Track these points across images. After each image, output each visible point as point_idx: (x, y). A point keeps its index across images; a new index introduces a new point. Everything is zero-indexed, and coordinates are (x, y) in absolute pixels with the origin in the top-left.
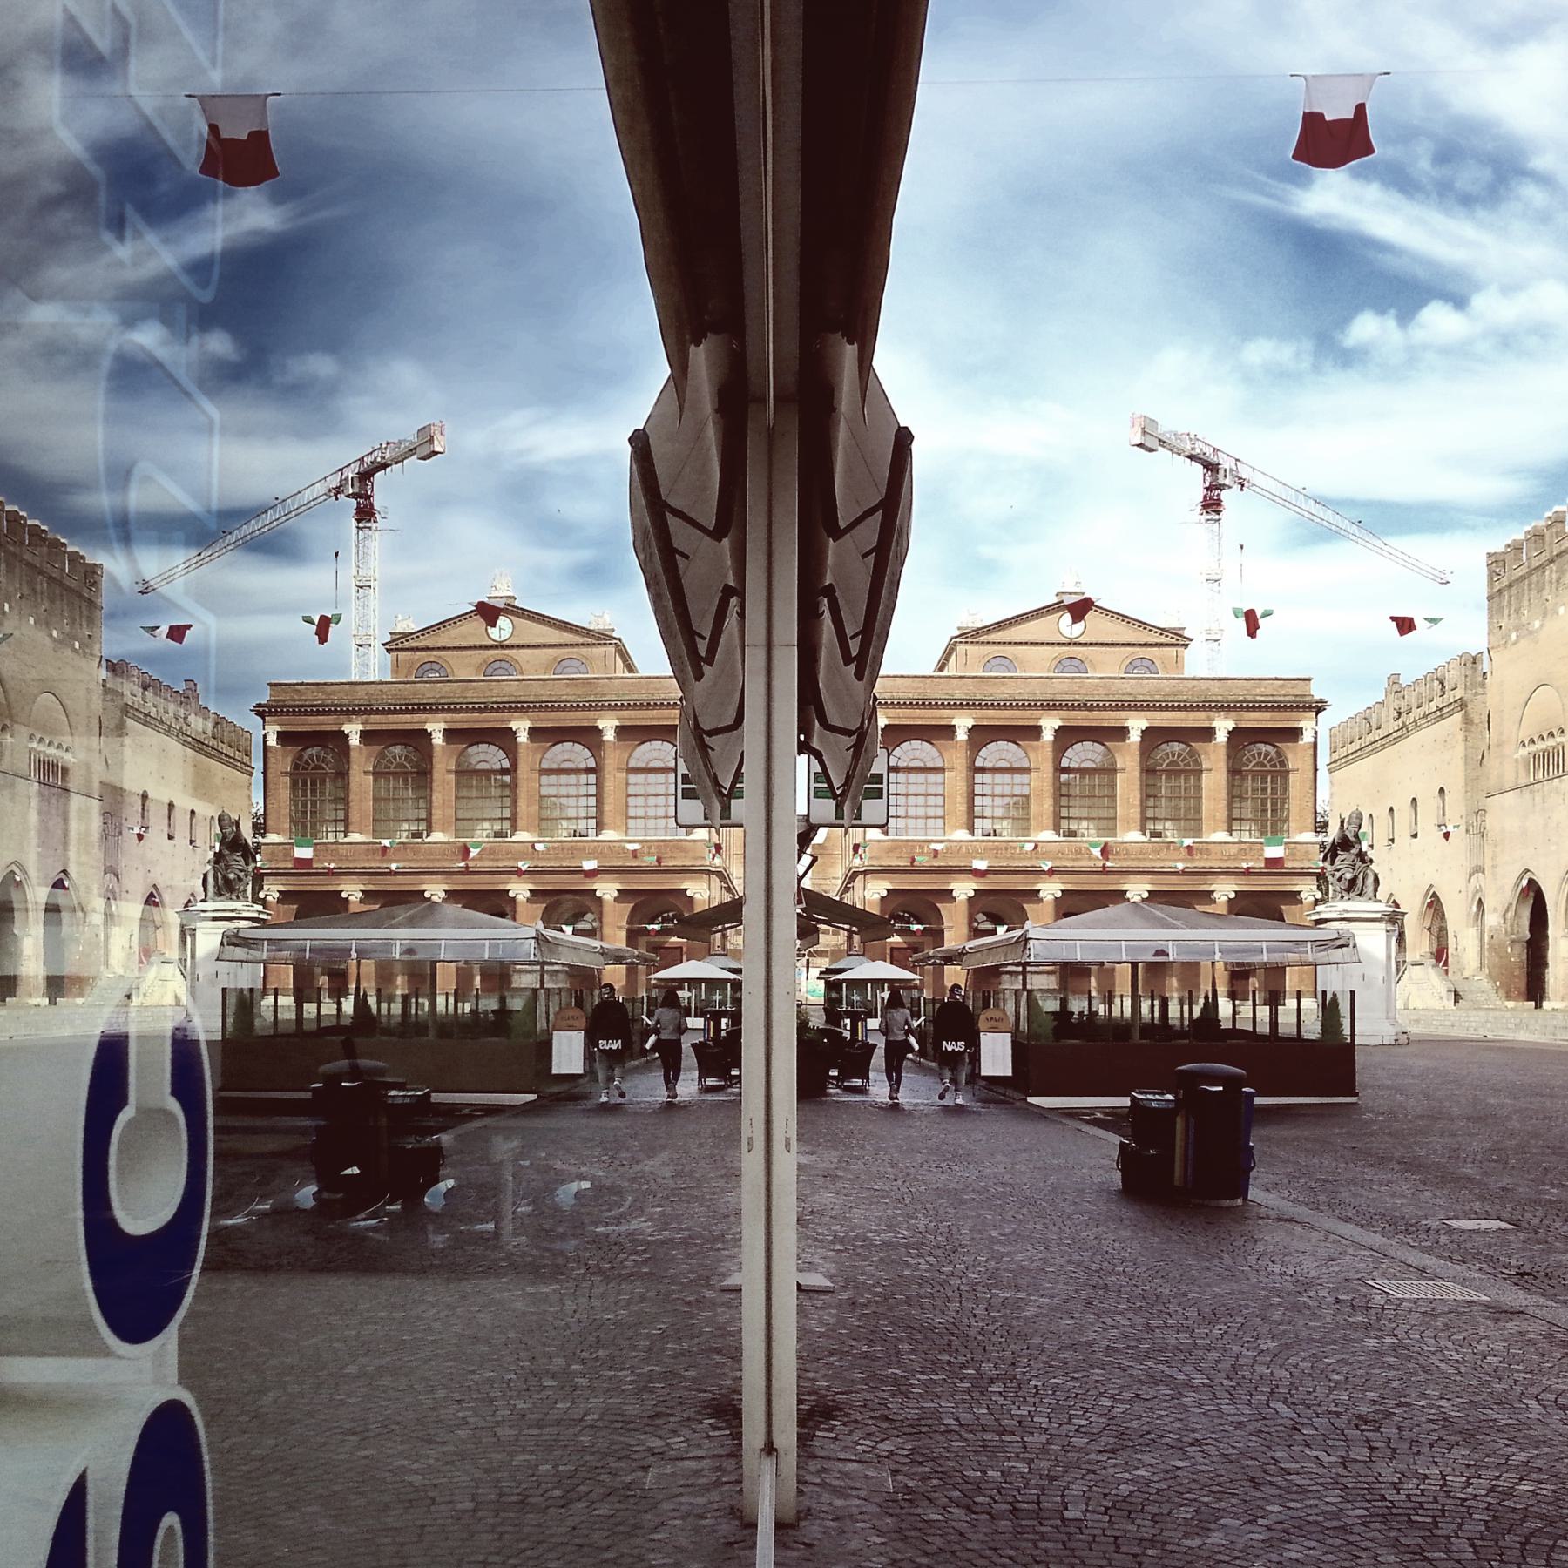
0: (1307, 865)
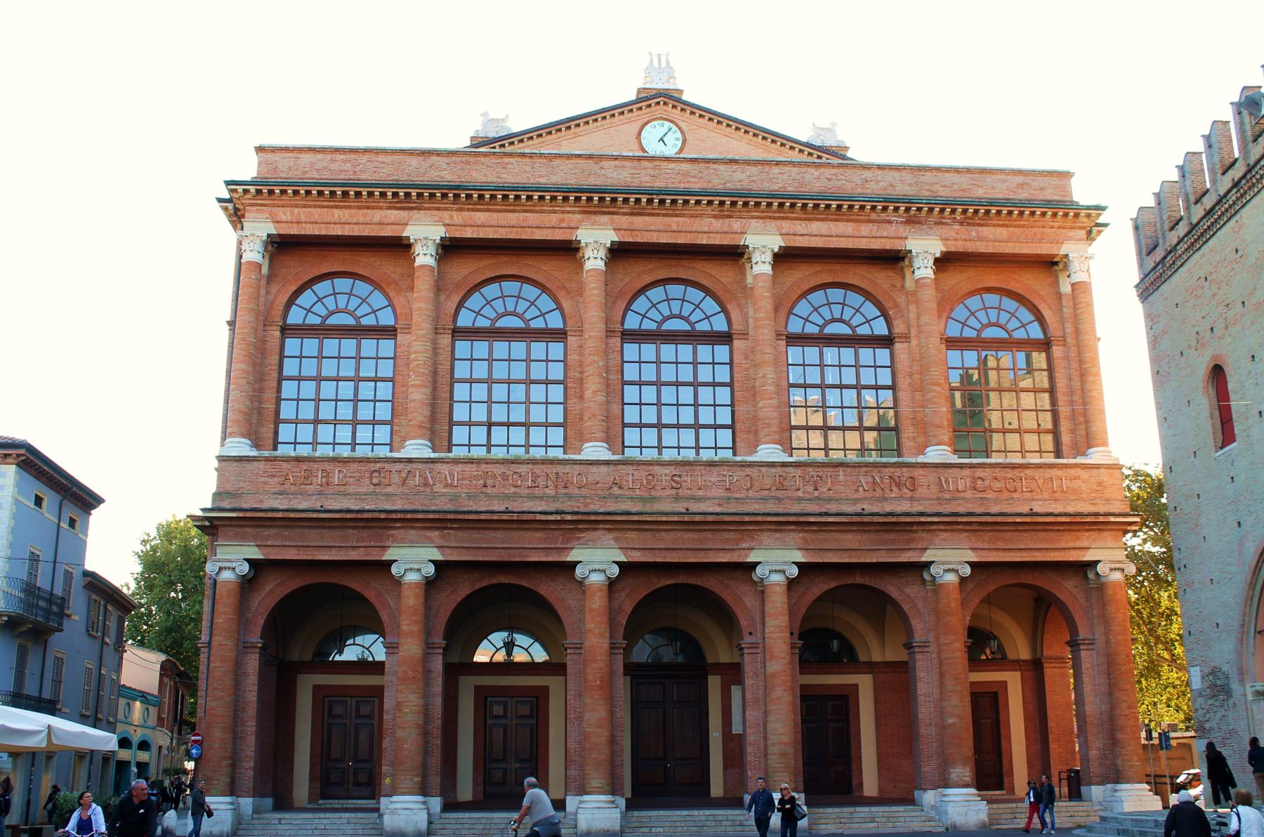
0: (1102, 510)
